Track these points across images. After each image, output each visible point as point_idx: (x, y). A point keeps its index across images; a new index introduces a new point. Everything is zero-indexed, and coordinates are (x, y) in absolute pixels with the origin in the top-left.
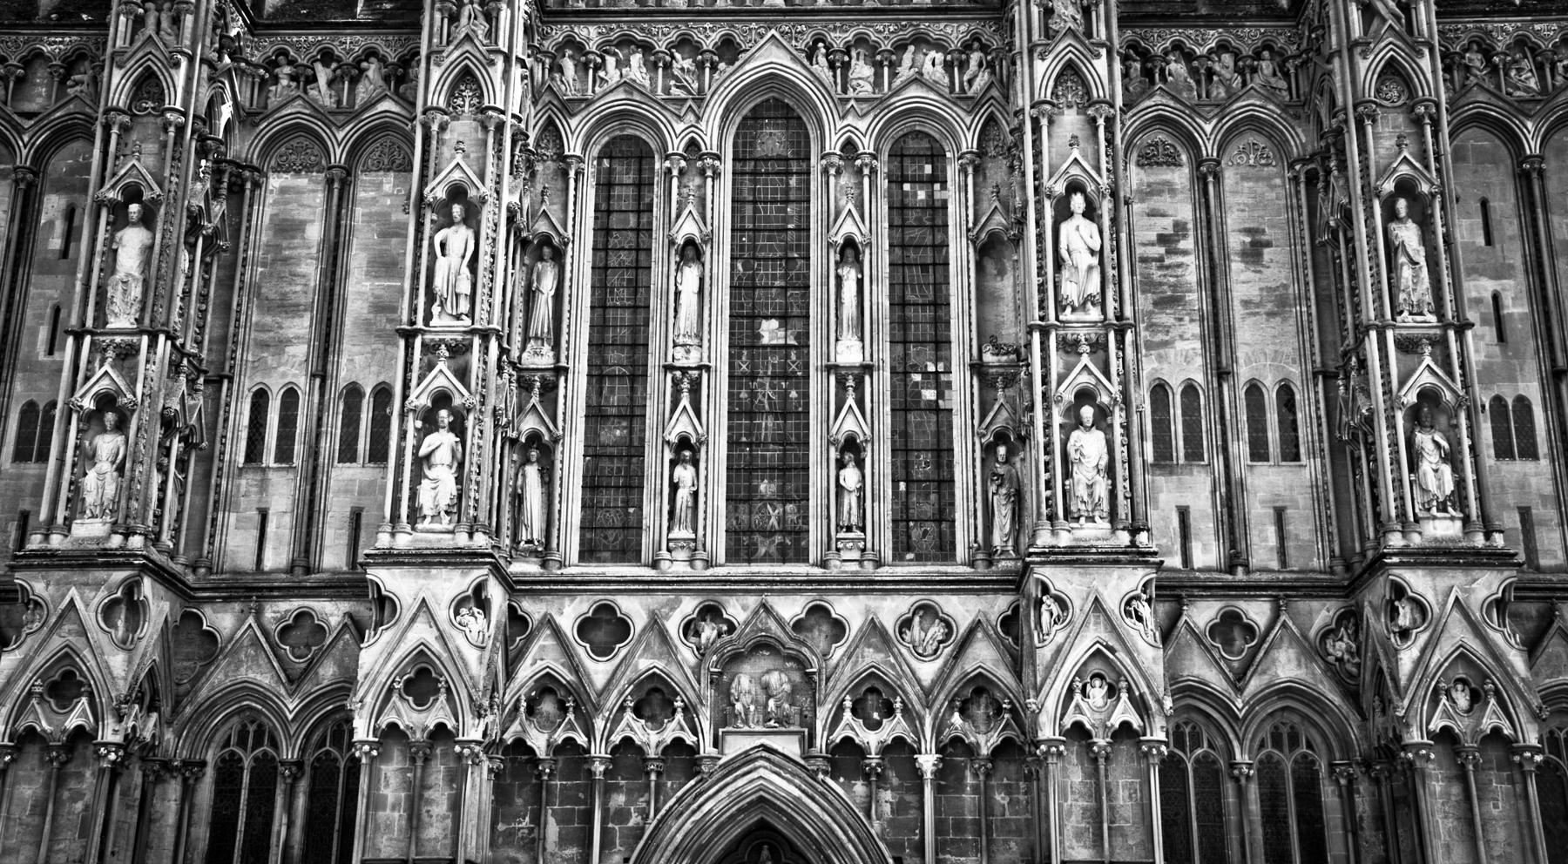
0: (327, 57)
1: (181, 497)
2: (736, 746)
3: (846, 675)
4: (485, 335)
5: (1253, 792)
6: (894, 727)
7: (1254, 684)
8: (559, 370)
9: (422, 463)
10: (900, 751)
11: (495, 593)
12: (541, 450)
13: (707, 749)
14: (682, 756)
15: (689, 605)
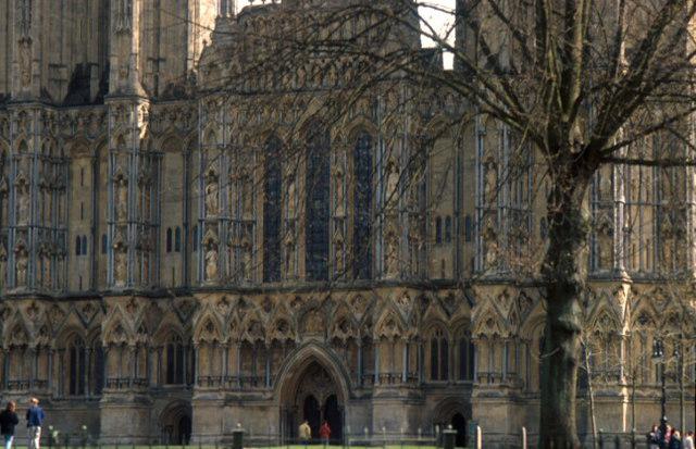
0: (179, 110)
1: (148, 266)
2: (306, 339)
3: (335, 319)
4: (222, 220)
5: (456, 349)
6: (350, 332)
7: (453, 317)
8: (255, 222)
9: (206, 261)
10: (350, 339)
11: (232, 298)
12: (248, 248)
13: (297, 340)
14: (289, 341)
15: (291, 296)
